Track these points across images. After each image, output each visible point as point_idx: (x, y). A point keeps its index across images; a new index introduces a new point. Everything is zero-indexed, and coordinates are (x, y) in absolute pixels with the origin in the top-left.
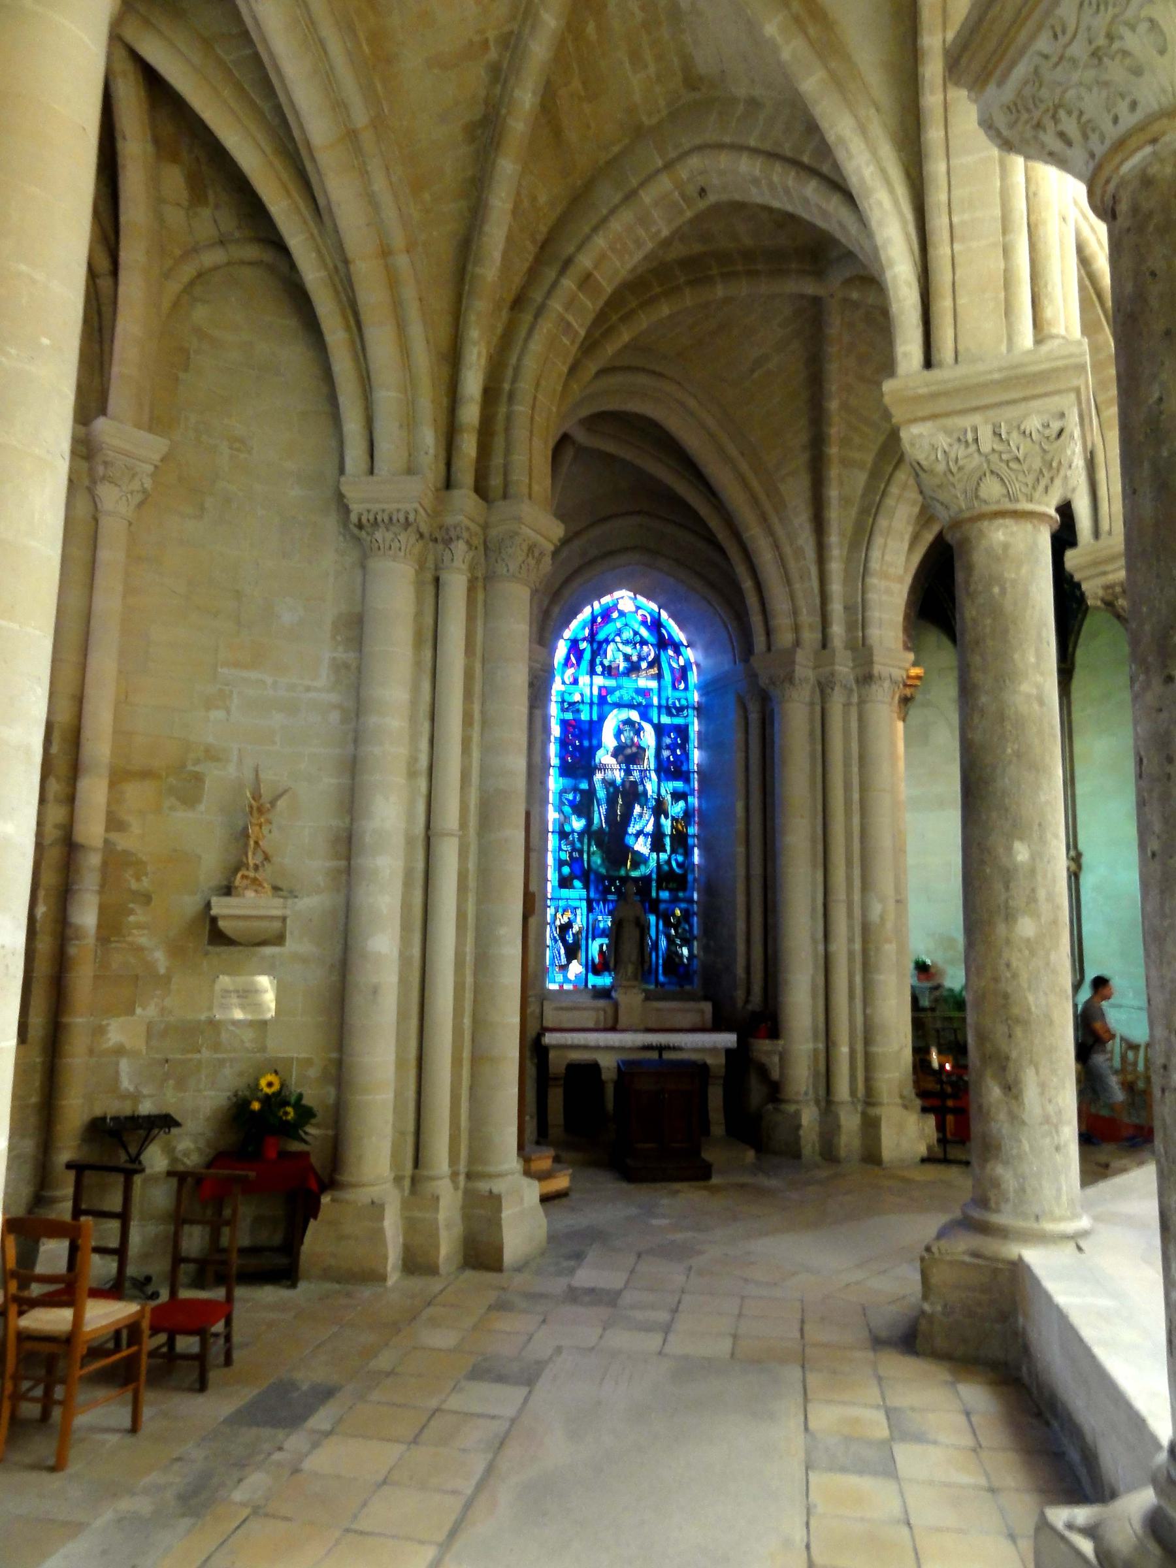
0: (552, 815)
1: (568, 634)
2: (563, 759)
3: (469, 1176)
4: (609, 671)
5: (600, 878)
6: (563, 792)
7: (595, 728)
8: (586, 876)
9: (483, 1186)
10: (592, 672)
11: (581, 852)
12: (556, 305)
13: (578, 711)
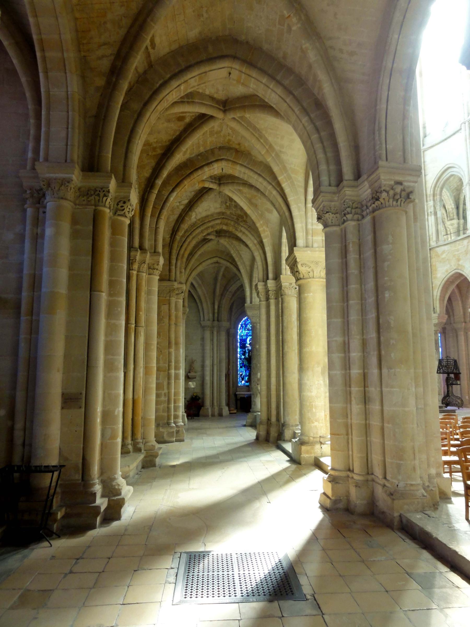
0: (239, 355)
1: (240, 323)
2: (240, 346)
3: (219, 406)
4: (248, 330)
5: (247, 366)
6: (240, 351)
7: (245, 340)
8: (245, 366)
9: (221, 407)
10: (245, 330)
11: (244, 362)
12: (226, 296)
13: (243, 337)
